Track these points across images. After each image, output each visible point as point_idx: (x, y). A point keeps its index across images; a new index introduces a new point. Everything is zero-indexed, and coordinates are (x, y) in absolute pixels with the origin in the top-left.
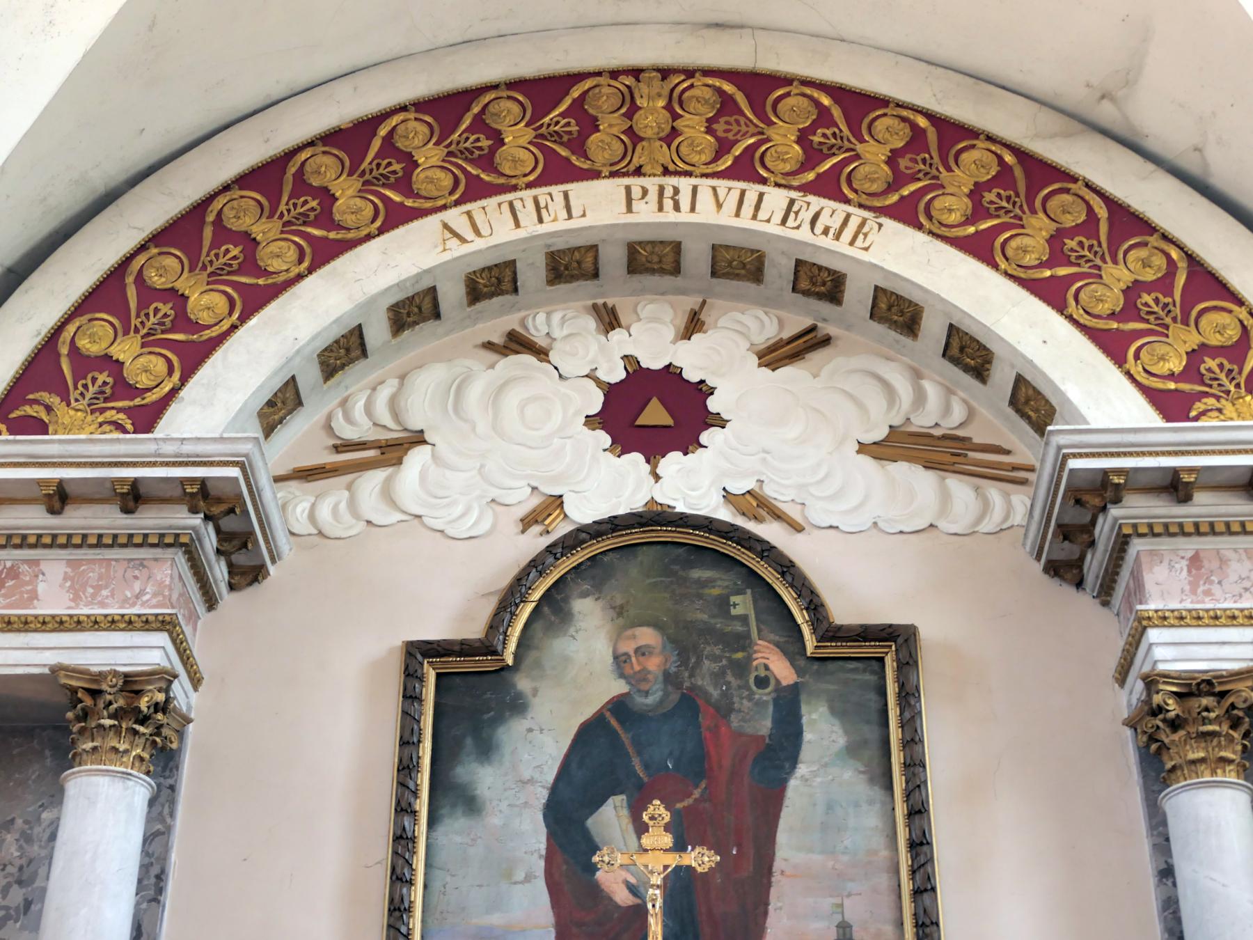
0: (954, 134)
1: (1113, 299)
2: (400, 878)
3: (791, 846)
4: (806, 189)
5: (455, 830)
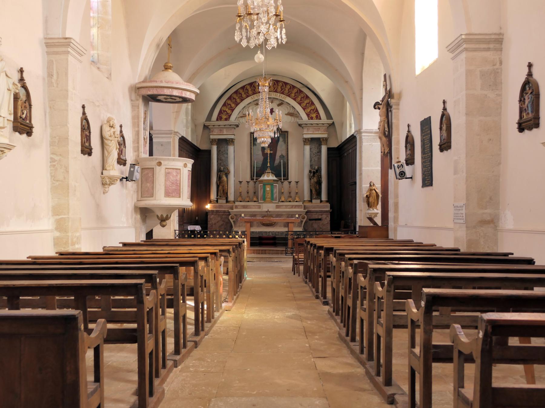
0: (294, 87)
1: (305, 105)
2: (251, 151)
3: (279, 148)
4: (282, 93)
5: (255, 147)
